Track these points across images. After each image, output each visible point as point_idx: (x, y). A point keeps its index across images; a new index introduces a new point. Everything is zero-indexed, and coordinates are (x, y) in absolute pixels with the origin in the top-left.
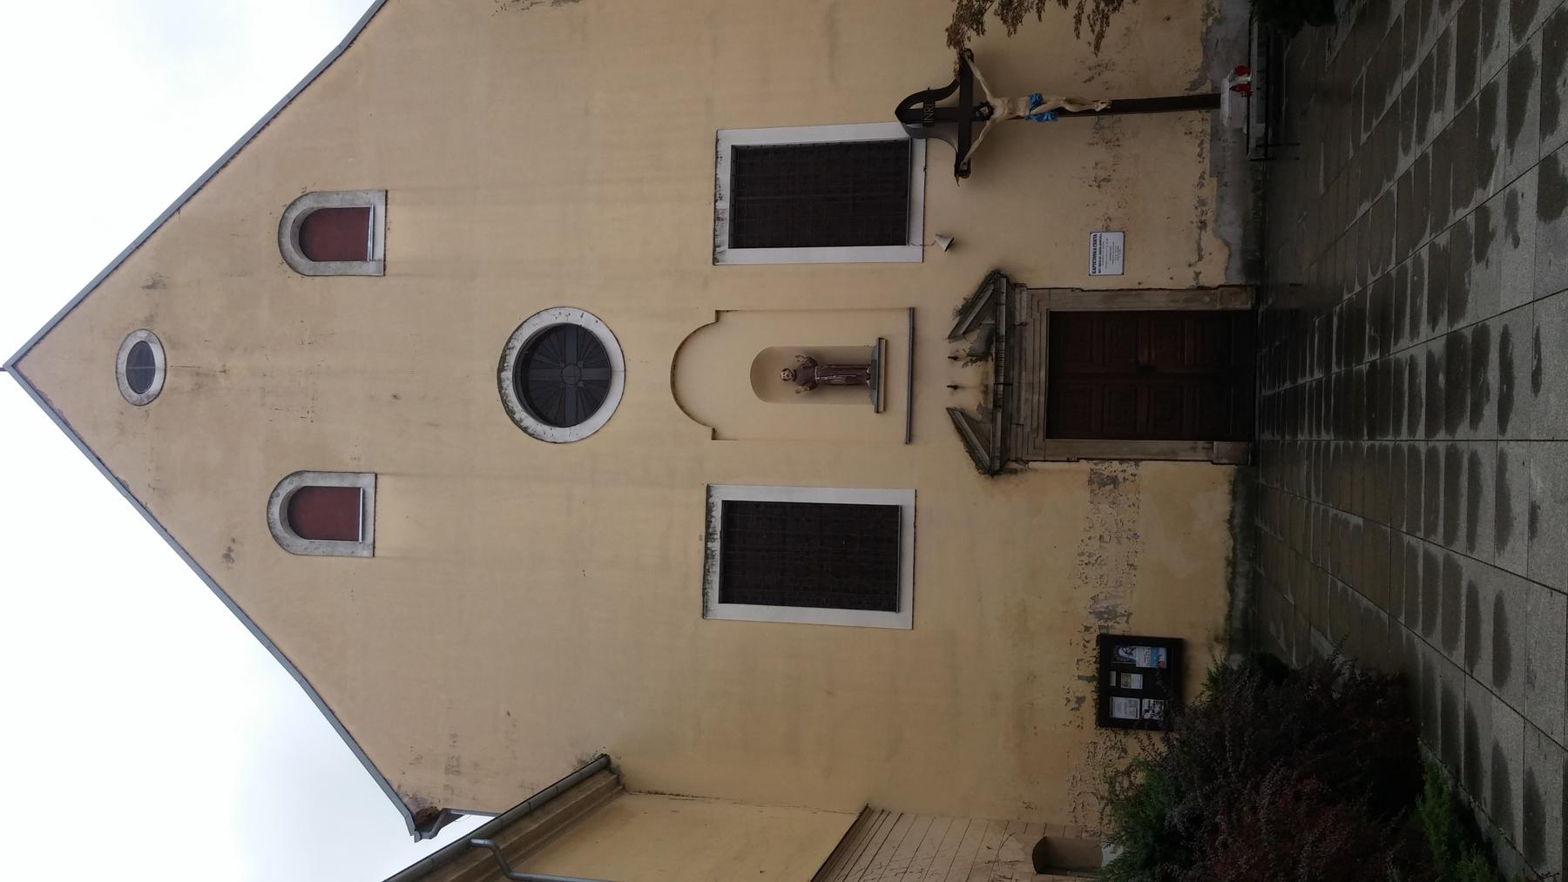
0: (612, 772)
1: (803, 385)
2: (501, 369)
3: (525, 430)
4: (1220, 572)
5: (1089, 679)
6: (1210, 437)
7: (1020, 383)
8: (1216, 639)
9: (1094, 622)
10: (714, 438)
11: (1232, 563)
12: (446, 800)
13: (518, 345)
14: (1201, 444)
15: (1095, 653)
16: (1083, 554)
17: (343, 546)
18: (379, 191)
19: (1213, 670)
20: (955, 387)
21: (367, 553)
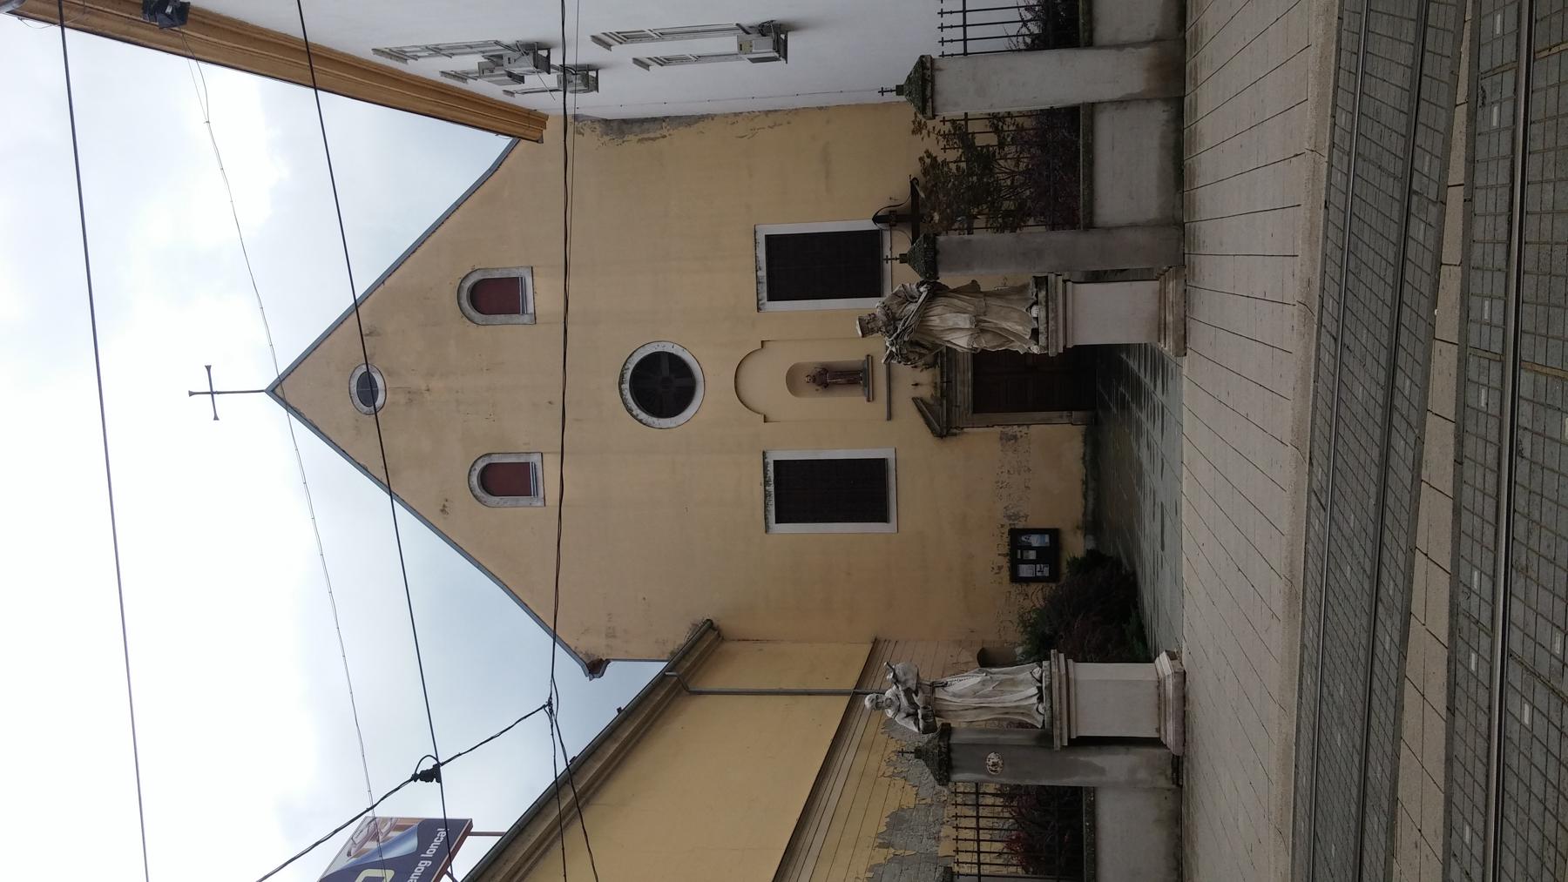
0: (715, 629)
1: (819, 385)
2: (621, 383)
3: (640, 421)
4: (1078, 488)
5: (1005, 555)
6: (1070, 409)
7: (956, 381)
8: (1078, 527)
9: (1007, 522)
10: (765, 422)
11: (1085, 483)
12: (608, 654)
13: (631, 366)
14: (1065, 413)
15: (1007, 540)
16: (998, 482)
17: (523, 500)
18: (527, 267)
19: (1069, 559)
20: (916, 385)
21: (539, 504)
